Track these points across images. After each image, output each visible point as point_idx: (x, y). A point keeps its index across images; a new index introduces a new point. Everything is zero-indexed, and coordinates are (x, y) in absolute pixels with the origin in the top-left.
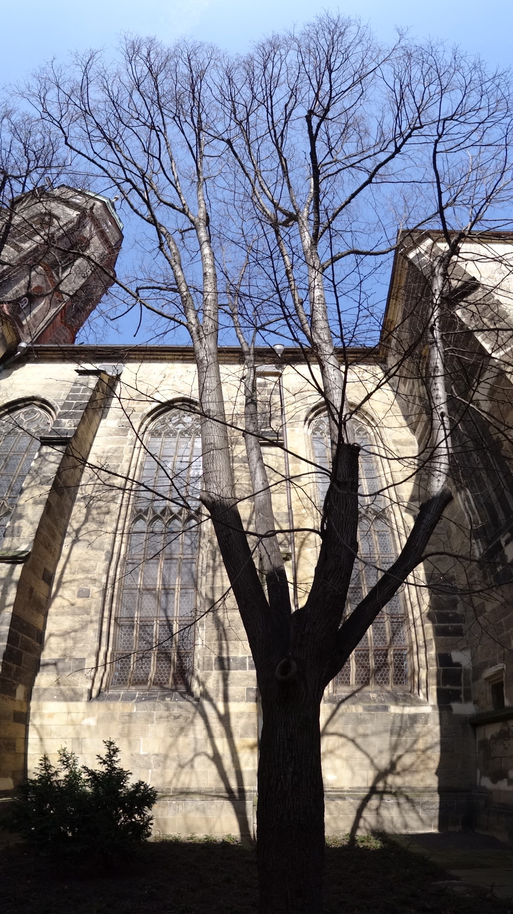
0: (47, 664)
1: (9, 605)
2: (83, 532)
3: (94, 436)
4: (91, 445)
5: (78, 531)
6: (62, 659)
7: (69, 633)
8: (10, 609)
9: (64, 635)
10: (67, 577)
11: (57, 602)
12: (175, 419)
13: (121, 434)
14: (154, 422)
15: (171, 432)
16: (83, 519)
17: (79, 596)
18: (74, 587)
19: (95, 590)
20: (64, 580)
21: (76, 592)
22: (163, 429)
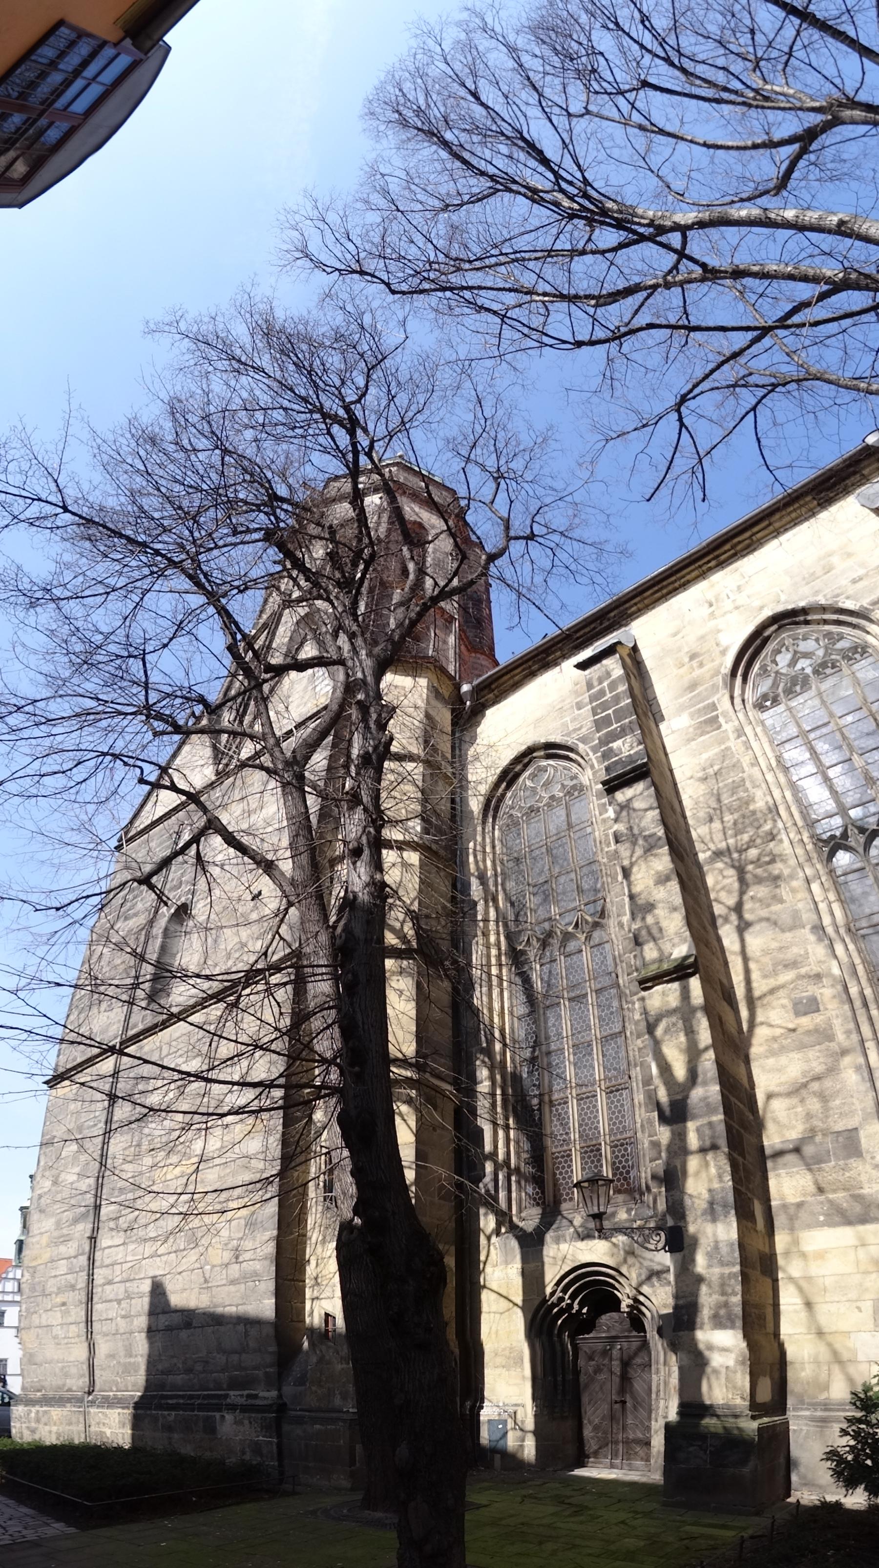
0: (779, 1154)
1: (706, 1049)
2: (748, 906)
3: (666, 754)
4: (671, 771)
5: (738, 908)
6: (810, 1136)
7: (805, 1085)
8: (711, 1055)
9: (797, 1090)
10: (760, 986)
11: (761, 1034)
12: (783, 660)
13: (708, 729)
14: (750, 683)
15: (794, 681)
16: (736, 885)
17: (798, 1013)
18: (783, 999)
19: (826, 993)
20: (757, 993)
21: (790, 1006)
22: (775, 685)
